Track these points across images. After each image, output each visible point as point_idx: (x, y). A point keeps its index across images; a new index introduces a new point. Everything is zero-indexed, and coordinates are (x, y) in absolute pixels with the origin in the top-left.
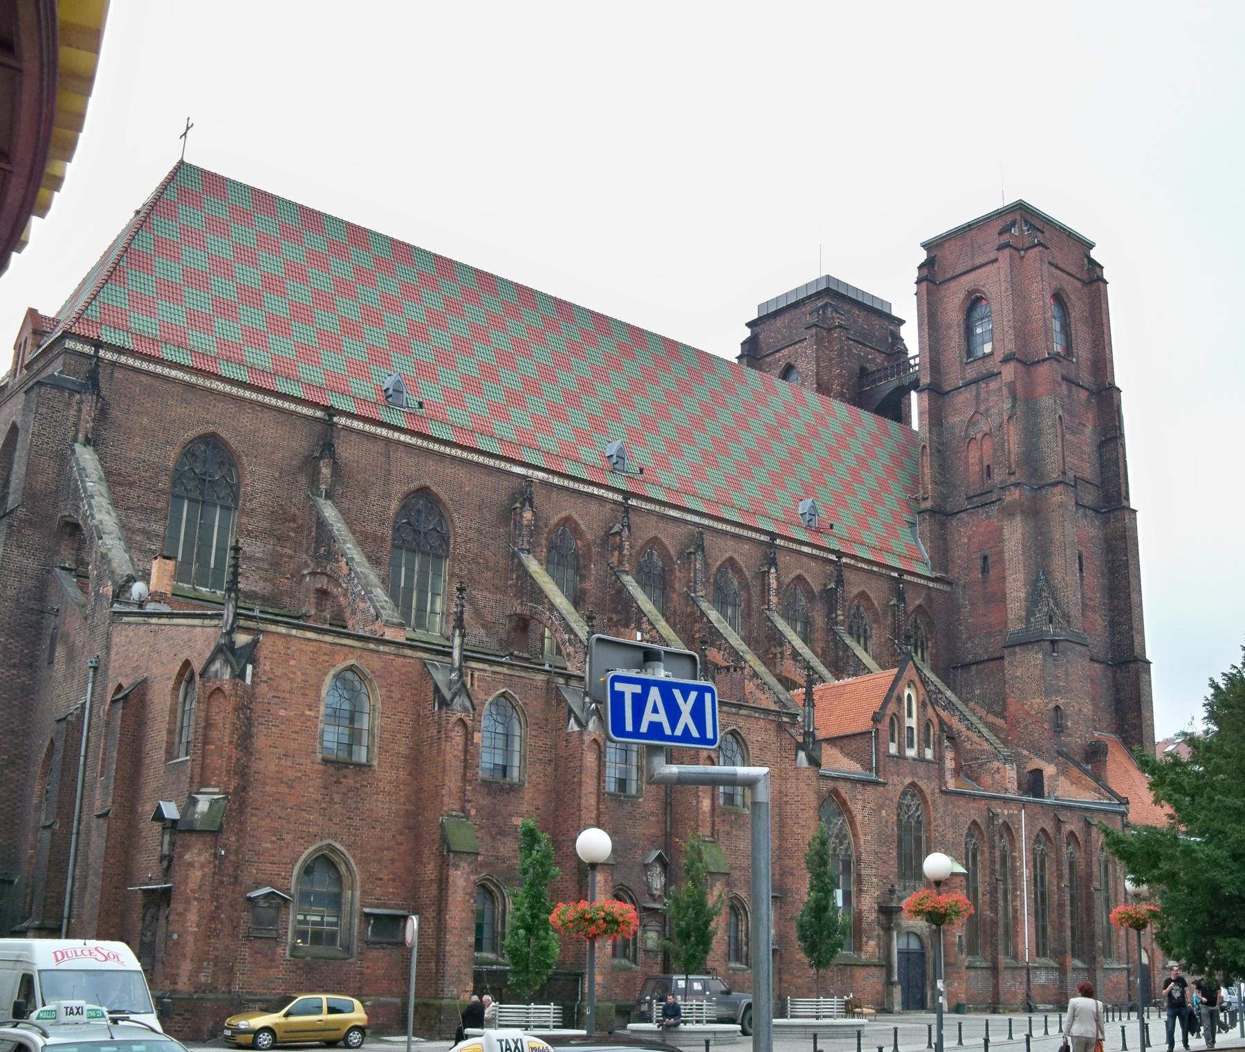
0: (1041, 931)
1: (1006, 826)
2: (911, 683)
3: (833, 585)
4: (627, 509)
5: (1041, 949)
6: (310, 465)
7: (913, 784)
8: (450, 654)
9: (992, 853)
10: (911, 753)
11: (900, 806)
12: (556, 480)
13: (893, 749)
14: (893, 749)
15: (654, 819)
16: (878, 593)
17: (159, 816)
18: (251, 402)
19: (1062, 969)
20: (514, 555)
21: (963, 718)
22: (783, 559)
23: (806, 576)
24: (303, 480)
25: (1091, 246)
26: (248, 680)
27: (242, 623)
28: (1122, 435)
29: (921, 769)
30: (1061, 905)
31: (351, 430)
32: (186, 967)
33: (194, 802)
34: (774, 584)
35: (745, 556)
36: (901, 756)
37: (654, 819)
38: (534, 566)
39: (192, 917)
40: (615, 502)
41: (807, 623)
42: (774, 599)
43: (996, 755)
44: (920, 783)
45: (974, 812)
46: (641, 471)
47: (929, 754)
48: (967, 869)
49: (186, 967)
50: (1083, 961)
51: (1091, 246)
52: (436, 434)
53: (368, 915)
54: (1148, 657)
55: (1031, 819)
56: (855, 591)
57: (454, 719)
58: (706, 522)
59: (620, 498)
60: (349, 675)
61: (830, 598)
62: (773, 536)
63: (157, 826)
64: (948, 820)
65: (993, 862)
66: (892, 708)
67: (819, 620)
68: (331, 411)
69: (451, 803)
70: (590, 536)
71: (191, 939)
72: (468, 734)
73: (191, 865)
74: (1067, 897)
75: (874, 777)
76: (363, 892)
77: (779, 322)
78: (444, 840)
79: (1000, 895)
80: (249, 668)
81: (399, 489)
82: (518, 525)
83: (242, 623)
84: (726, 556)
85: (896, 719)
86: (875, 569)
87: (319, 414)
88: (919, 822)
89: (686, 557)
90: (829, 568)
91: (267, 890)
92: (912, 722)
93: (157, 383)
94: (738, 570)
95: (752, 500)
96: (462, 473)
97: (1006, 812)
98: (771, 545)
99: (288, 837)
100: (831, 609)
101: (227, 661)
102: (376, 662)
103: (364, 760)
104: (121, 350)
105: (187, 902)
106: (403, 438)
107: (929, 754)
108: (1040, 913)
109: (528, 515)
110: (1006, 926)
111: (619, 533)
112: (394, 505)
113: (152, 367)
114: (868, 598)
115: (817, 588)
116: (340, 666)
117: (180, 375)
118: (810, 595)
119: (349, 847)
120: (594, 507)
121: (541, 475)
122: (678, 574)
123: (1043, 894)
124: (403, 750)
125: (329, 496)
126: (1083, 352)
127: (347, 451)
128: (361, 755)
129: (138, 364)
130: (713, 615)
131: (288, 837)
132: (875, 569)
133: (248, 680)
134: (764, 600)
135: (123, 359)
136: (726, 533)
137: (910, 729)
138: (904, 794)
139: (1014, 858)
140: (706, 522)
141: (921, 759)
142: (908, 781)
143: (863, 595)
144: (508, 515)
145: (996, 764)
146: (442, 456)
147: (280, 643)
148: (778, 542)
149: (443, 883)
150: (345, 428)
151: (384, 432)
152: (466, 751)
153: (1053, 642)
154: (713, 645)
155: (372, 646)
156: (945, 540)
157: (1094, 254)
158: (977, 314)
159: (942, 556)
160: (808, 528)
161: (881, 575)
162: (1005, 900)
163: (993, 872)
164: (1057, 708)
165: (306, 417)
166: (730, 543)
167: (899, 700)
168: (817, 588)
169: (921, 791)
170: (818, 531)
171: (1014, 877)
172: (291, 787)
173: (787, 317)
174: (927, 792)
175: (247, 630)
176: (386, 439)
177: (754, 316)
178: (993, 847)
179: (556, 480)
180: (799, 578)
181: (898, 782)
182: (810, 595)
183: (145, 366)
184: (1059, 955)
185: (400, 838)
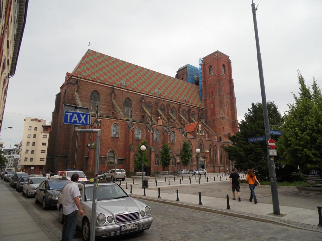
0: (221, 161)
1: (215, 145)
2: (200, 124)
3: (189, 110)
4: (158, 99)
5: (221, 163)
6: (111, 94)
7: (201, 139)
8: (130, 121)
9: (213, 149)
10: (200, 134)
11: (199, 142)
12: (148, 96)
14: (198, 134)
15: (161, 144)
16: (196, 111)
17: (87, 146)
19: (225, 167)
20: (142, 107)
21: (209, 129)
22: (182, 106)
24: (110, 97)
25: (229, 57)
26: (100, 126)
27: (99, 117)
28: (233, 86)
29: (202, 137)
30: (224, 157)
32: (91, 168)
33: (92, 144)
34: (180, 110)
35: (176, 106)
36: (199, 135)
37: (161, 144)
38: (144, 108)
39: (92, 161)
40: (156, 99)
41: (185, 115)
42: (180, 112)
43: (214, 135)
44: (202, 139)
45: (210, 143)
46: (160, 94)
47: (203, 134)
48: (209, 151)
49: (91, 168)
50: (228, 165)
51: (229, 57)
53: (119, 159)
54: (238, 120)
55: (219, 144)
56: (192, 111)
57: (131, 130)
58: (170, 101)
59: (157, 98)
60: (115, 124)
61: (189, 112)
62: (180, 103)
63: (87, 147)
64: (206, 144)
65: (213, 150)
66: (197, 128)
67: (187, 115)
68: (113, 86)
69: (130, 143)
70: (153, 104)
71: (92, 164)
72: (133, 133)
73: (91, 153)
74: (225, 156)
75: (195, 138)
76: (118, 156)
77: (181, 71)
78: (130, 148)
79: (215, 155)
80: (100, 124)
81: (125, 98)
82: (142, 102)
83: (99, 117)
84: (173, 106)
85: (198, 129)
87: (112, 87)
88: (202, 145)
89: (167, 106)
90: (188, 108)
91: (103, 156)
92: (201, 130)
93: (83, 82)
94: (175, 108)
95: (172, 96)
96: (134, 95)
99: (106, 148)
100: (189, 113)
101: (96, 123)
102: (119, 123)
103: (118, 137)
104: (81, 78)
105: (91, 158)
106: (124, 90)
107: (203, 134)
108: (221, 159)
109: (143, 101)
110: (216, 160)
111: (157, 103)
112: (124, 100)
113: (86, 80)
115: (187, 110)
116: (114, 123)
117: (90, 81)
118: (186, 112)
119: (115, 149)
120: (153, 99)
121: (145, 95)
122: (166, 109)
123: (221, 155)
124: (124, 135)
125: (114, 99)
126: (227, 74)
127: (116, 92)
128: (117, 136)
129: (84, 80)
130: (171, 115)
131: (106, 148)
133: (100, 126)
134: (179, 112)
135: (81, 79)
136: (172, 103)
137: (200, 131)
138: (200, 140)
139: (217, 150)
140: (170, 101)
142: (200, 138)
143: (193, 111)
144: (141, 101)
145: (214, 136)
146: (131, 92)
147: (105, 120)
148: (181, 104)
149: (129, 154)
150: (116, 89)
151: (122, 89)
152: (133, 135)
153: (223, 118)
154: (171, 119)
155: (119, 120)
156: (206, 103)
157: (229, 58)
158: (211, 69)
159: (206, 105)
160: (185, 102)
162: (215, 156)
163: (213, 152)
164: (223, 127)
165: (110, 87)
166: (174, 104)
167: (199, 126)
168: (187, 110)
169: (202, 140)
170: (187, 102)
171: (217, 153)
172: (107, 141)
173: (182, 70)
175: (100, 118)
177: (177, 71)
178: (213, 148)
179: (148, 96)
180: (184, 109)
181: (198, 139)
182: (186, 112)
183: (85, 80)
184: (224, 165)
185: (123, 148)
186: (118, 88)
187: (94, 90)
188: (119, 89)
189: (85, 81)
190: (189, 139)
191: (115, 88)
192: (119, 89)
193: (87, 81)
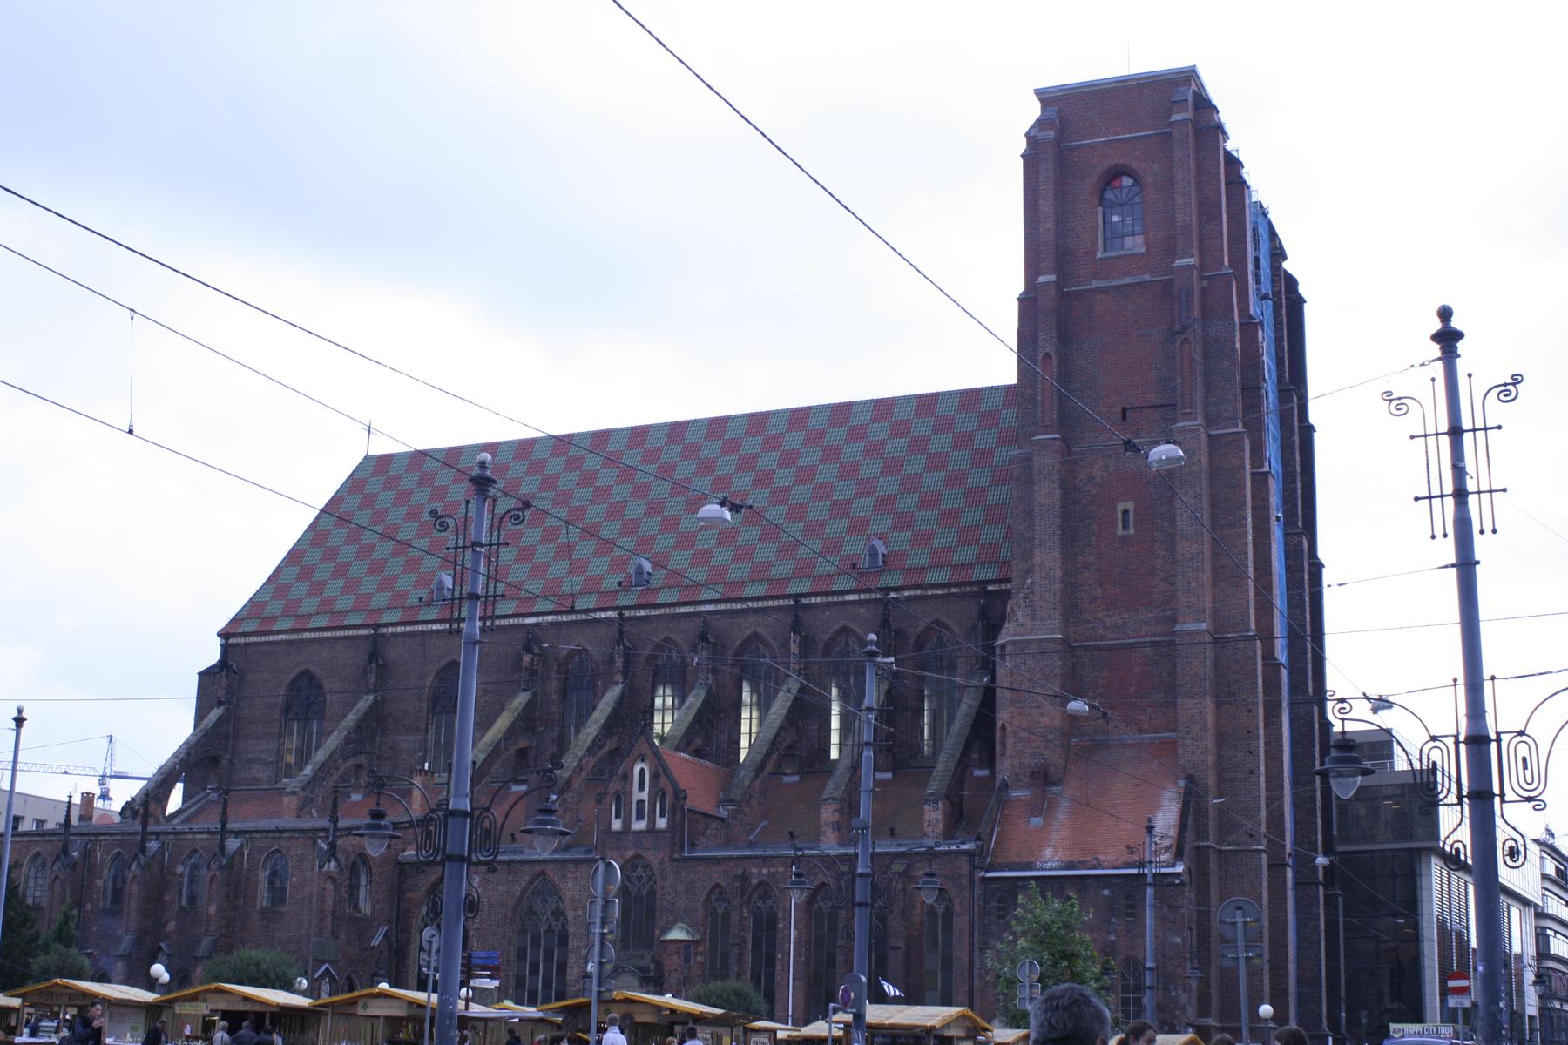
7: (637, 856)
10: (639, 826)
12: (564, 618)
13: (616, 825)
18: (328, 639)
23: (852, 625)
31: (395, 635)
52: (426, 618)
58: (722, 607)
64: (680, 888)
86: (953, 590)
92: (645, 796)
97: (765, 871)
98: (798, 607)
114: (947, 627)
121: (550, 618)
127: (393, 653)
132: (953, 590)
140: (722, 607)
141: (651, 829)
142: (630, 853)
148: (804, 601)
151: (420, 628)
161: (964, 594)
174: (655, 863)
176: (422, 633)
179: (564, 618)
186: (400, 629)
187: (297, 671)
188: (408, 629)
189: (266, 643)
190: (538, 868)
191: (391, 630)
192: (408, 629)
193: (271, 638)
